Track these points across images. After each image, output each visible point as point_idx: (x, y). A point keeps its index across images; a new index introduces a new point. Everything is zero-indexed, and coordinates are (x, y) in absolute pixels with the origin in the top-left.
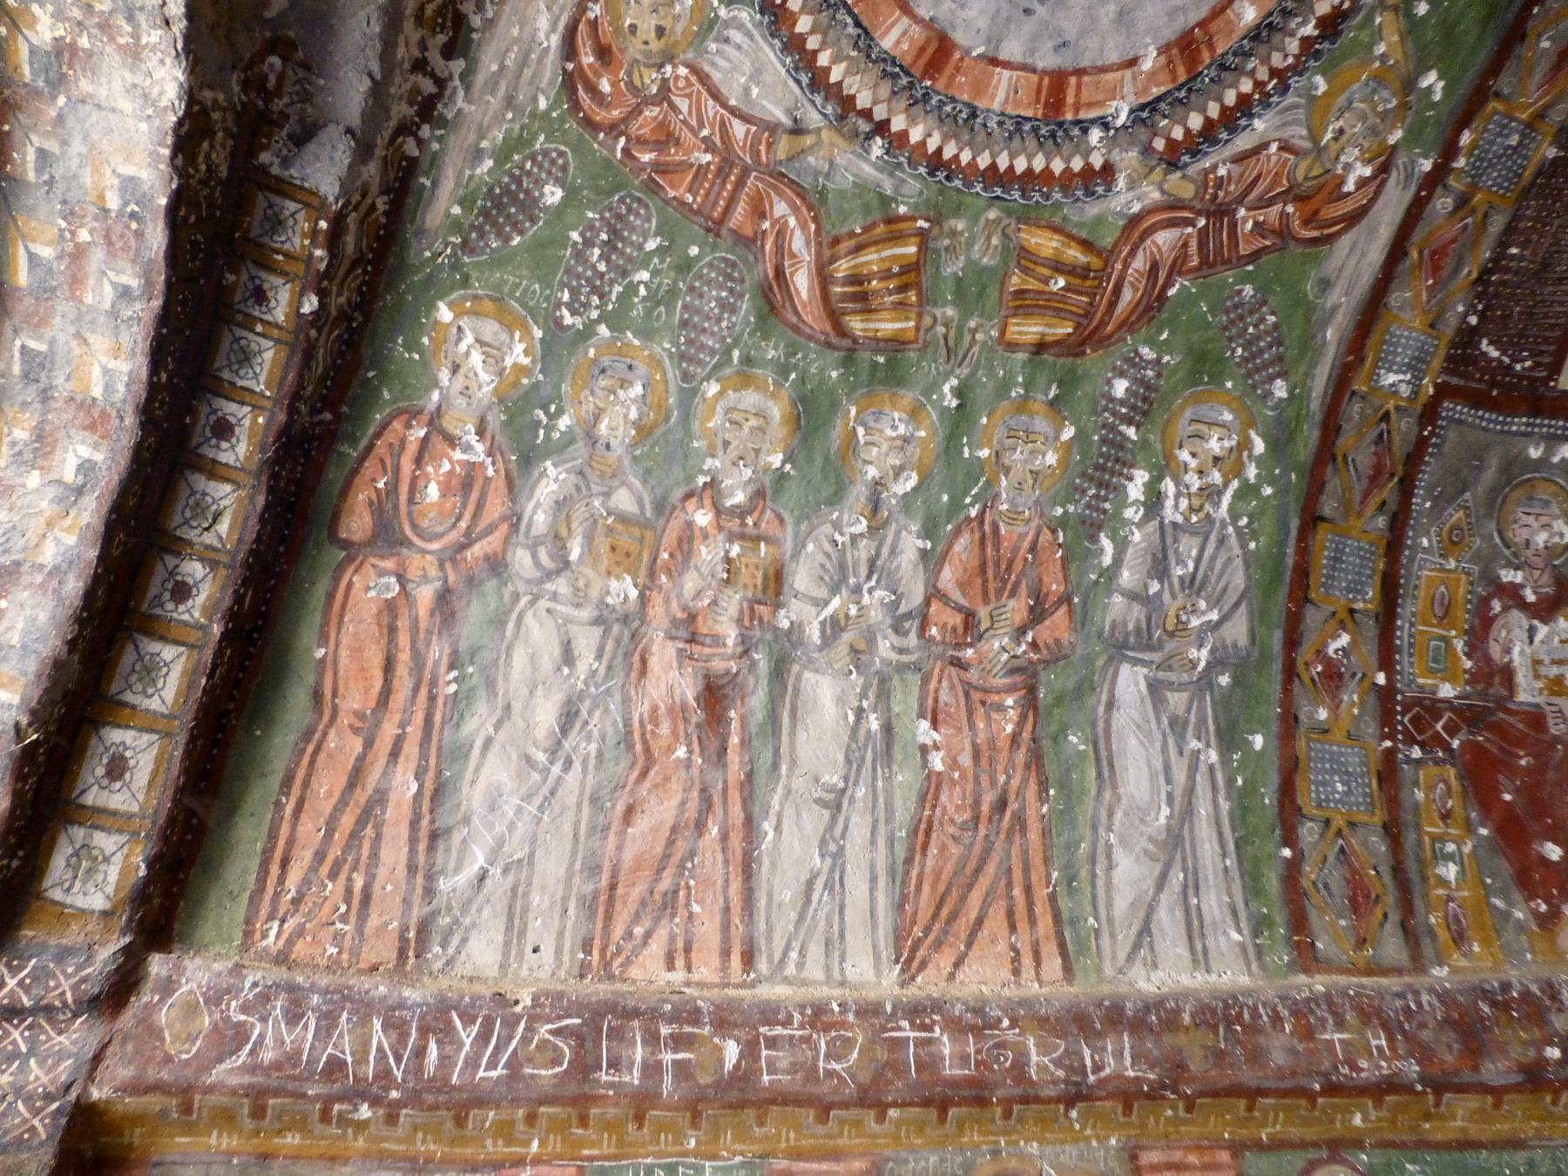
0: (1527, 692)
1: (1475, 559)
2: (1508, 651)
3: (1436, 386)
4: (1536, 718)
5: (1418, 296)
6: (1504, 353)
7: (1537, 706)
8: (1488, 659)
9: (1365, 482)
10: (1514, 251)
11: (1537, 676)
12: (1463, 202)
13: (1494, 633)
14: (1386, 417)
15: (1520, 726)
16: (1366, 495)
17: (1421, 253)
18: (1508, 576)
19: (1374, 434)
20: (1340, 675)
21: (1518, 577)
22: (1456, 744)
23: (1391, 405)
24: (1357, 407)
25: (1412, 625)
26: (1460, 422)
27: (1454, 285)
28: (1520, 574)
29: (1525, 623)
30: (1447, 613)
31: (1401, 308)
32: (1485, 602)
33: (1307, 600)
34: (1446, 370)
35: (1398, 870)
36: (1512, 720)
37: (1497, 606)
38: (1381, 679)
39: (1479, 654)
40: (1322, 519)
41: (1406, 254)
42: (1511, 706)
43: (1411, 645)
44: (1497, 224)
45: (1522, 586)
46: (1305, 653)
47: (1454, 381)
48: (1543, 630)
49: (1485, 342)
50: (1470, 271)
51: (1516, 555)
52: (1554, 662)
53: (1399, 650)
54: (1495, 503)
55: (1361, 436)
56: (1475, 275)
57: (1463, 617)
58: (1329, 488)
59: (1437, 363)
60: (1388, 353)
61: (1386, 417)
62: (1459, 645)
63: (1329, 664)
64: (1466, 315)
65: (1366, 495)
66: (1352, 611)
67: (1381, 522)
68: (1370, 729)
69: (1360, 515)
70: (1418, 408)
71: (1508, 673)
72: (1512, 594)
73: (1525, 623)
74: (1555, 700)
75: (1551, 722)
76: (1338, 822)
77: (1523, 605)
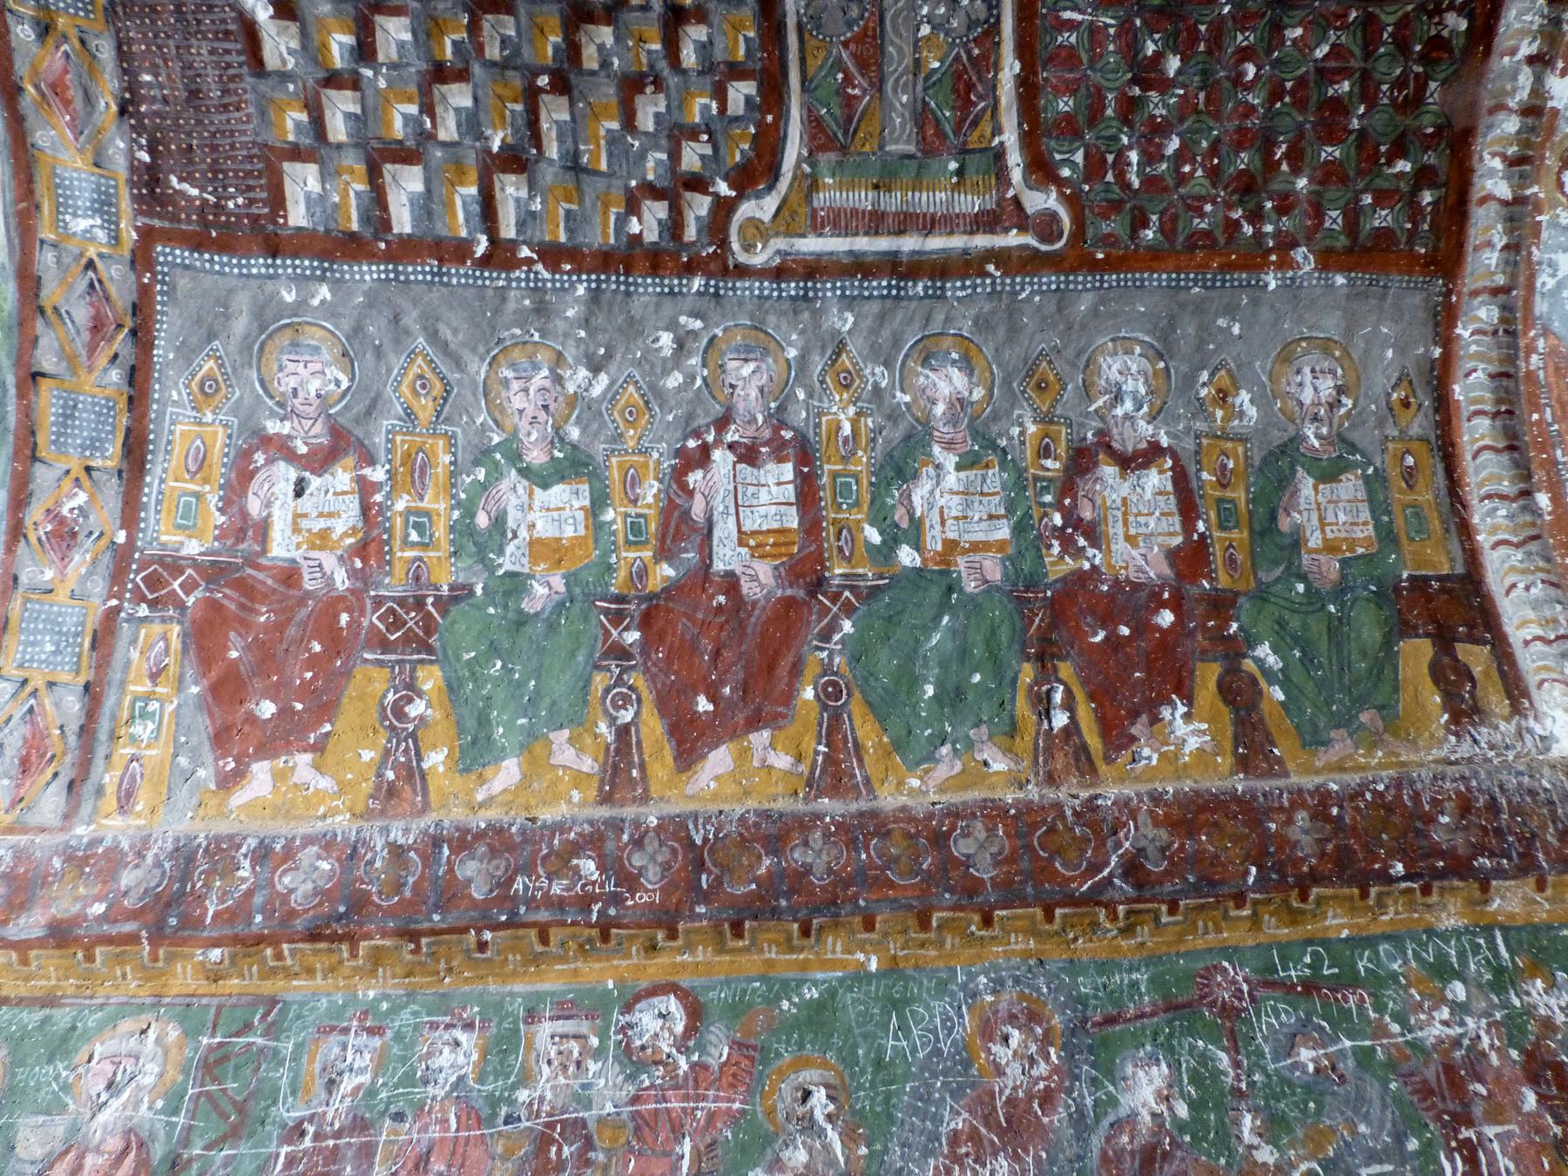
0: (281, 546)
1: (234, 411)
2: (268, 505)
3: (137, 229)
4: (290, 575)
5: (62, 136)
6: (203, 189)
7: (293, 561)
8: (244, 514)
9: (86, 336)
10: (147, 78)
11: (296, 530)
12: (45, 29)
13: (254, 485)
14: (90, 265)
15: (270, 582)
16: (92, 349)
17: (37, 87)
18: (273, 427)
19: (82, 285)
20: (74, 535)
21: (286, 428)
22: (190, 601)
23: (92, 252)
24: (49, 256)
25: (162, 481)
26: (187, 267)
27: (98, 119)
28: (287, 424)
29: (293, 474)
30: (200, 468)
31: (54, 147)
32: (246, 455)
33: (34, 458)
34: (140, 212)
35: (87, 731)
36: (261, 576)
37: (260, 458)
38: (121, 537)
39: (235, 509)
40: (43, 375)
41: (21, 89)
42: (263, 561)
43: (159, 502)
44: (106, 51)
45: (289, 436)
46: (35, 513)
47: (157, 223)
48: (315, 482)
49: (174, 180)
50: (107, 104)
51: (281, 405)
52: (321, 515)
53: (145, 507)
54: (255, 350)
55: (71, 287)
56: (114, 108)
57: (218, 471)
58: (43, 342)
59: (126, 205)
60: (66, 197)
61: (90, 265)
62: (213, 500)
63: (61, 521)
64: (131, 152)
65: (92, 349)
66: (88, 469)
67: (115, 375)
68: (99, 586)
69: (90, 370)
70: (127, 254)
71: (263, 530)
72: (281, 449)
73: (293, 474)
74: (314, 554)
75: (306, 577)
76: (38, 681)
77: (291, 457)
